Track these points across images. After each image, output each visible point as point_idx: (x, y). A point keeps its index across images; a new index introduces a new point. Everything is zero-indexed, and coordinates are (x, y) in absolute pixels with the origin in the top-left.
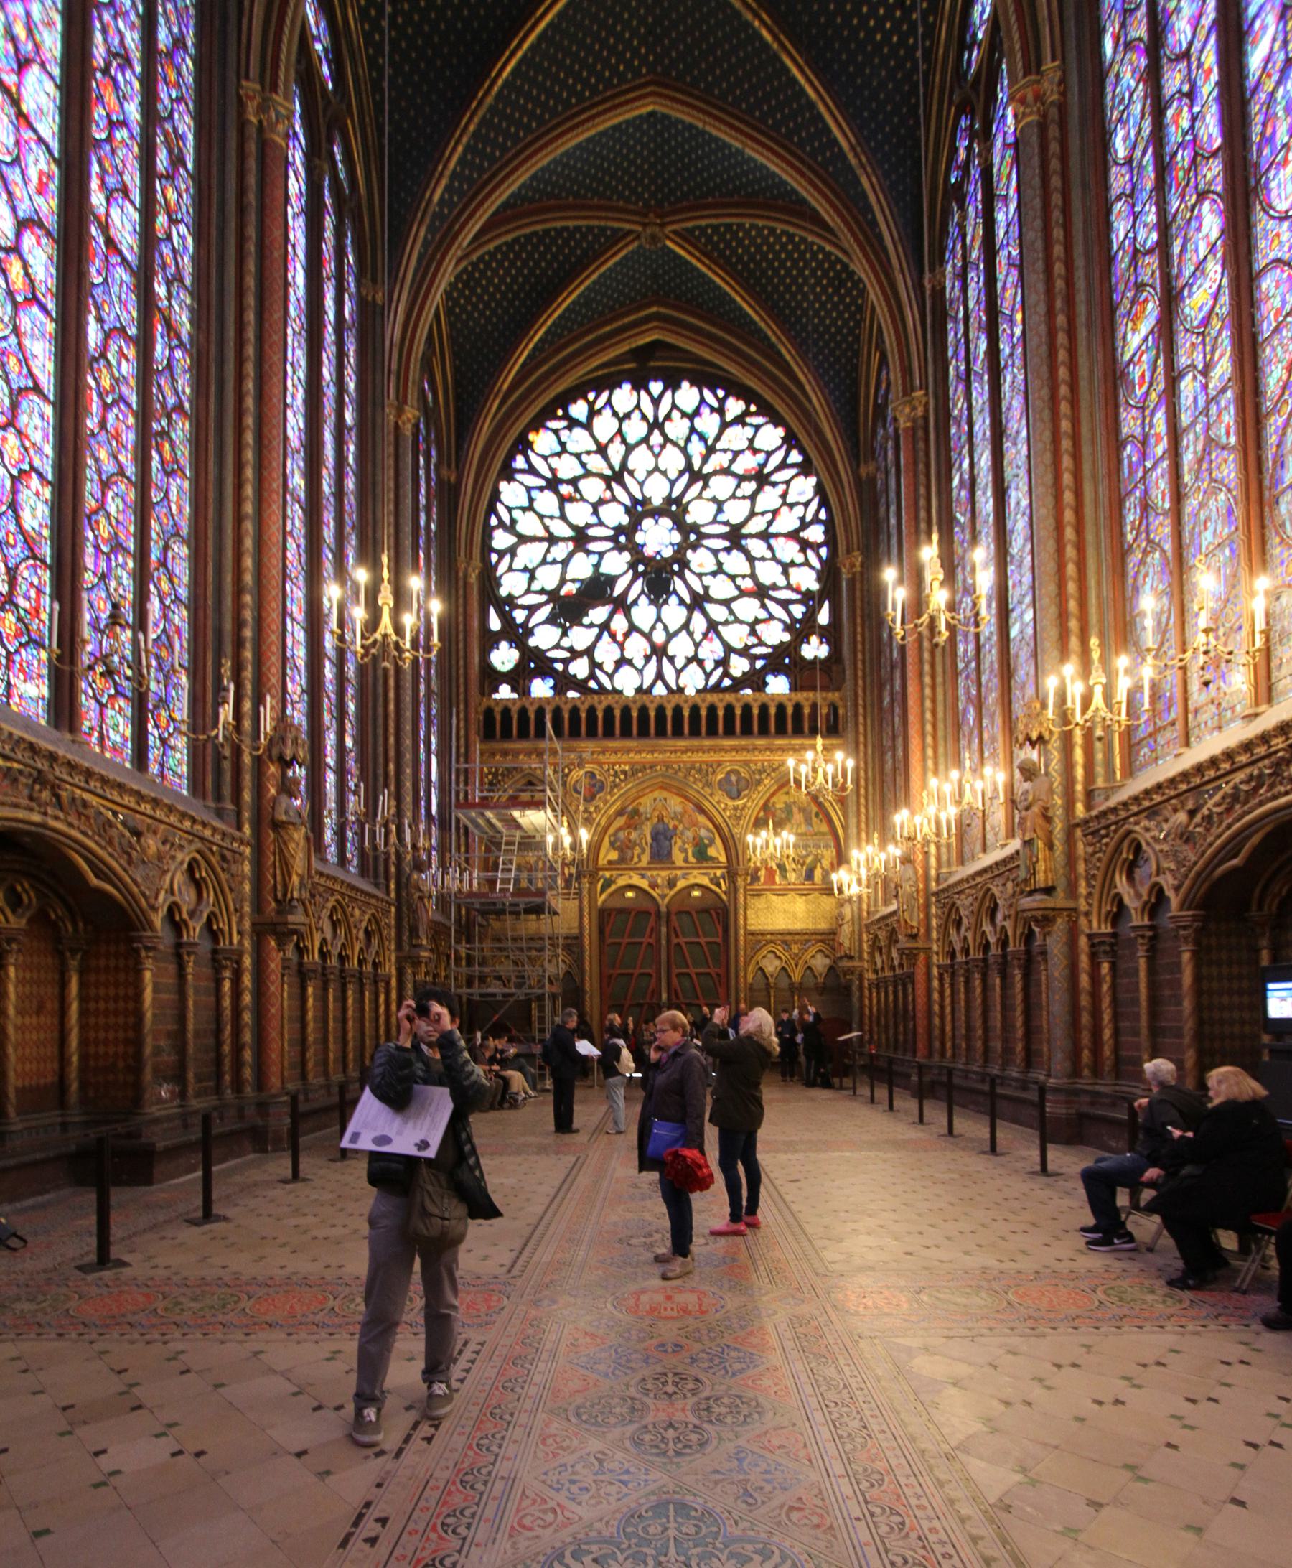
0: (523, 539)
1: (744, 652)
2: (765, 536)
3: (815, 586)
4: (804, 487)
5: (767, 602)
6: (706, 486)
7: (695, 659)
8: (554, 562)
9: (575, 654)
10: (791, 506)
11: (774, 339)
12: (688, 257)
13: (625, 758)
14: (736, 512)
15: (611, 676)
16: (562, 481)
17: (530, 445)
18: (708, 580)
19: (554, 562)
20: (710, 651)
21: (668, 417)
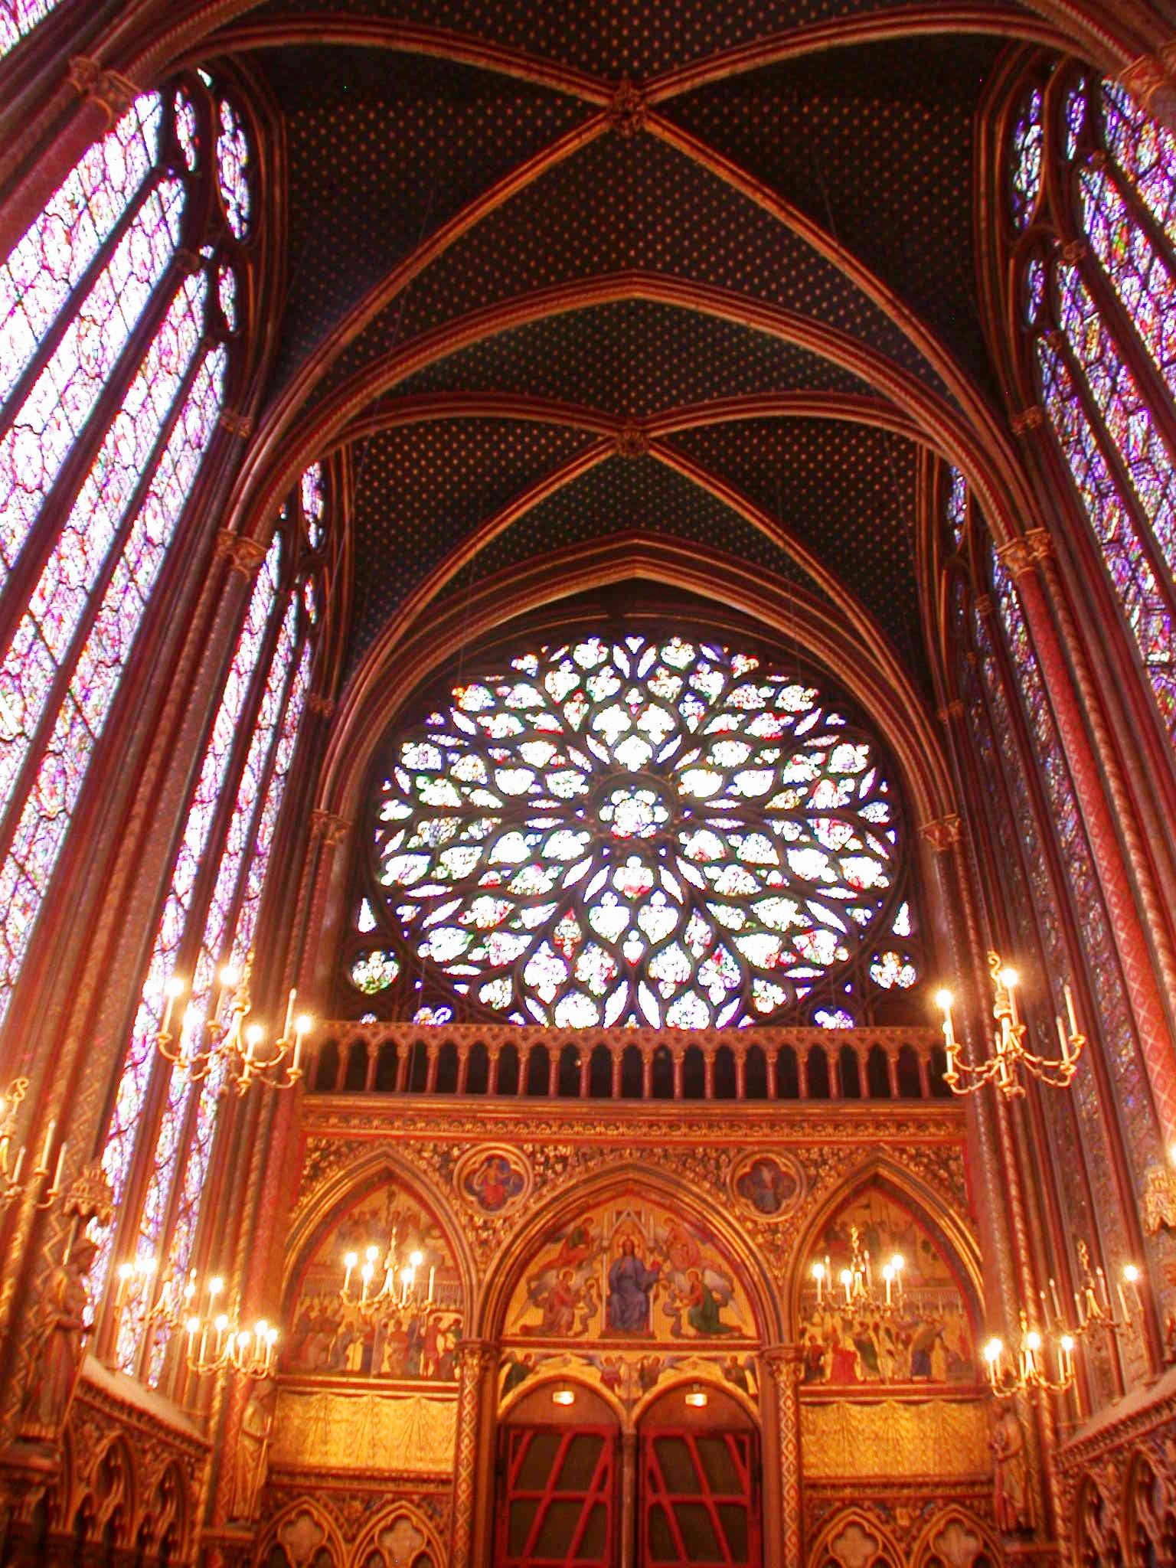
1: (776, 974)
2: (801, 814)
3: (884, 882)
5: (809, 903)
6: (707, 751)
7: (691, 985)
9: (490, 972)
10: (837, 778)
11: (797, 559)
12: (678, 469)
13: (566, 1132)
14: (753, 784)
17: (454, 701)
18: (712, 872)
19: (472, 842)
20: (719, 977)
21: (651, 674)
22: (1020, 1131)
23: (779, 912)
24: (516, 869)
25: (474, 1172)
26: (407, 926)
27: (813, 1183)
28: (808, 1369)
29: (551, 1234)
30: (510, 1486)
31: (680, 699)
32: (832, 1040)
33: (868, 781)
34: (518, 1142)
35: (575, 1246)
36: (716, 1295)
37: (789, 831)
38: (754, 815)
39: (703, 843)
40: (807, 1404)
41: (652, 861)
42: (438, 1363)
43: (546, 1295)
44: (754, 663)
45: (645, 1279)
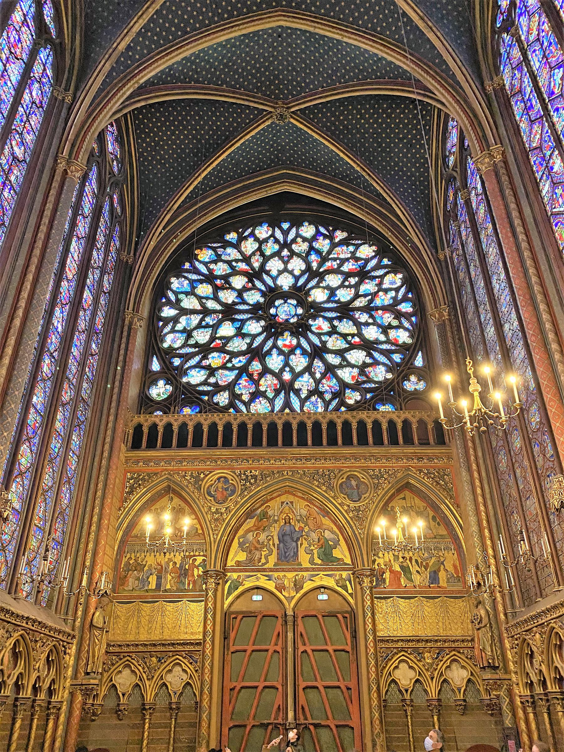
0: (185, 312)
1: (355, 387)
4: (394, 280)
6: (322, 279)
7: (315, 392)
8: (207, 326)
9: (218, 388)
10: (386, 291)
11: (367, 177)
13: (255, 464)
14: (344, 295)
15: (247, 404)
16: (217, 277)
17: (196, 257)
19: (207, 326)
21: (294, 241)
22: (481, 461)
23: (357, 356)
24: (227, 339)
25: (211, 485)
26: (177, 368)
27: (377, 487)
28: (377, 579)
29: (249, 515)
30: (231, 644)
31: (308, 254)
32: (384, 417)
33: (403, 290)
34: (233, 469)
35: (261, 520)
36: (331, 543)
37: (364, 318)
38: (345, 311)
39: (320, 324)
40: (376, 598)
41: (294, 334)
42: (194, 582)
43: (247, 545)
44: (345, 235)
45: (295, 536)
